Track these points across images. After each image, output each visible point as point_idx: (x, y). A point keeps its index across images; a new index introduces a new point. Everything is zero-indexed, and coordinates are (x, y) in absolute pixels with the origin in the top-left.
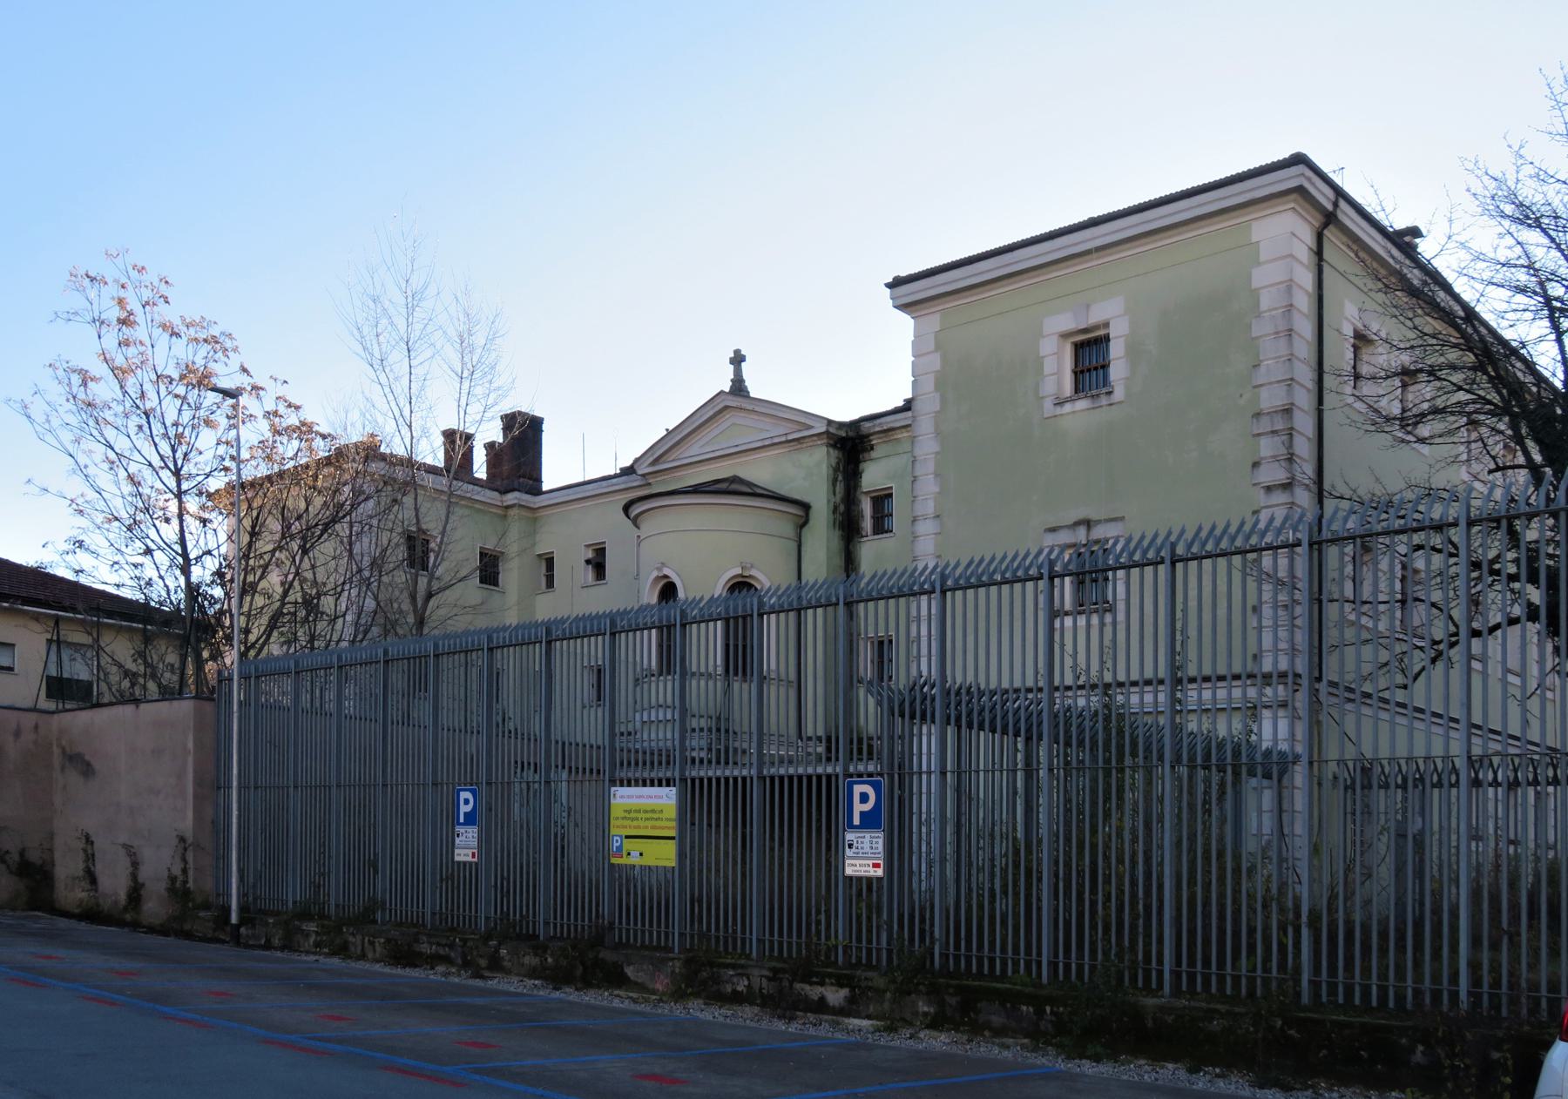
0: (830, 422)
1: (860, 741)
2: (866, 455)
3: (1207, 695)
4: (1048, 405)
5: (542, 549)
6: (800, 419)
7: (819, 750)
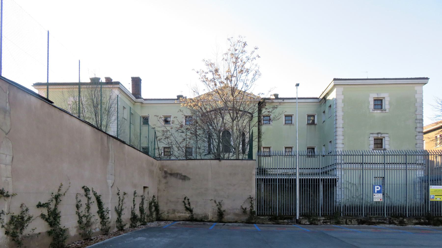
3: (400, 166)
4: (371, 111)
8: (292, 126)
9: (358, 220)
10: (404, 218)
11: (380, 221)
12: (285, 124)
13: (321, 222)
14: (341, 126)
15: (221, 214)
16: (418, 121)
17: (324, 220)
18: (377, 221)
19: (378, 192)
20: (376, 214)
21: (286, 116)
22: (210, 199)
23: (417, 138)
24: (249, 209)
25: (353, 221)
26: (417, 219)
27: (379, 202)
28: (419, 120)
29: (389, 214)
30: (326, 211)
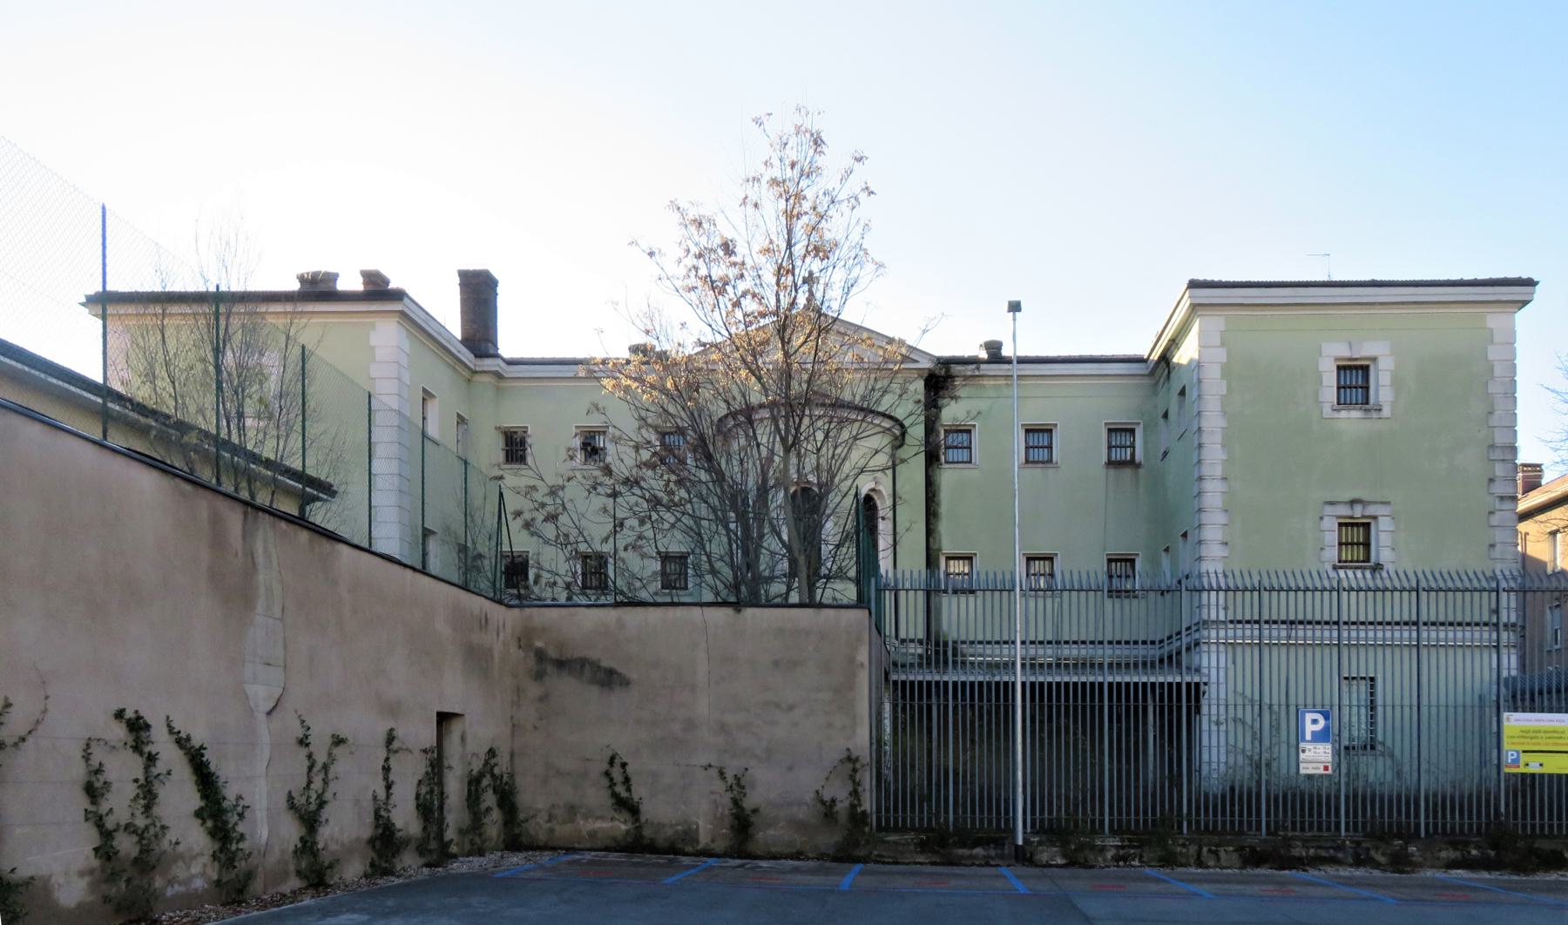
5: (512, 422)
6: (910, 354)
8: (1051, 472)
9: (1242, 848)
10: (1407, 843)
11: (1323, 853)
12: (1027, 461)
13: (1109, 855)
14: (1218, 471)
15: (742, 823)
16: (1497, 455)
17: (1117, 847)
18: (1312, 851)
20: (1311, 824)
22: (704, 762)
23: (1495, 520)
24: (847, 803)
25: (1222, 854)
26: (1454, 845)
28: (1504, 448)
29: (1356, 824)
30: (1128, 814)
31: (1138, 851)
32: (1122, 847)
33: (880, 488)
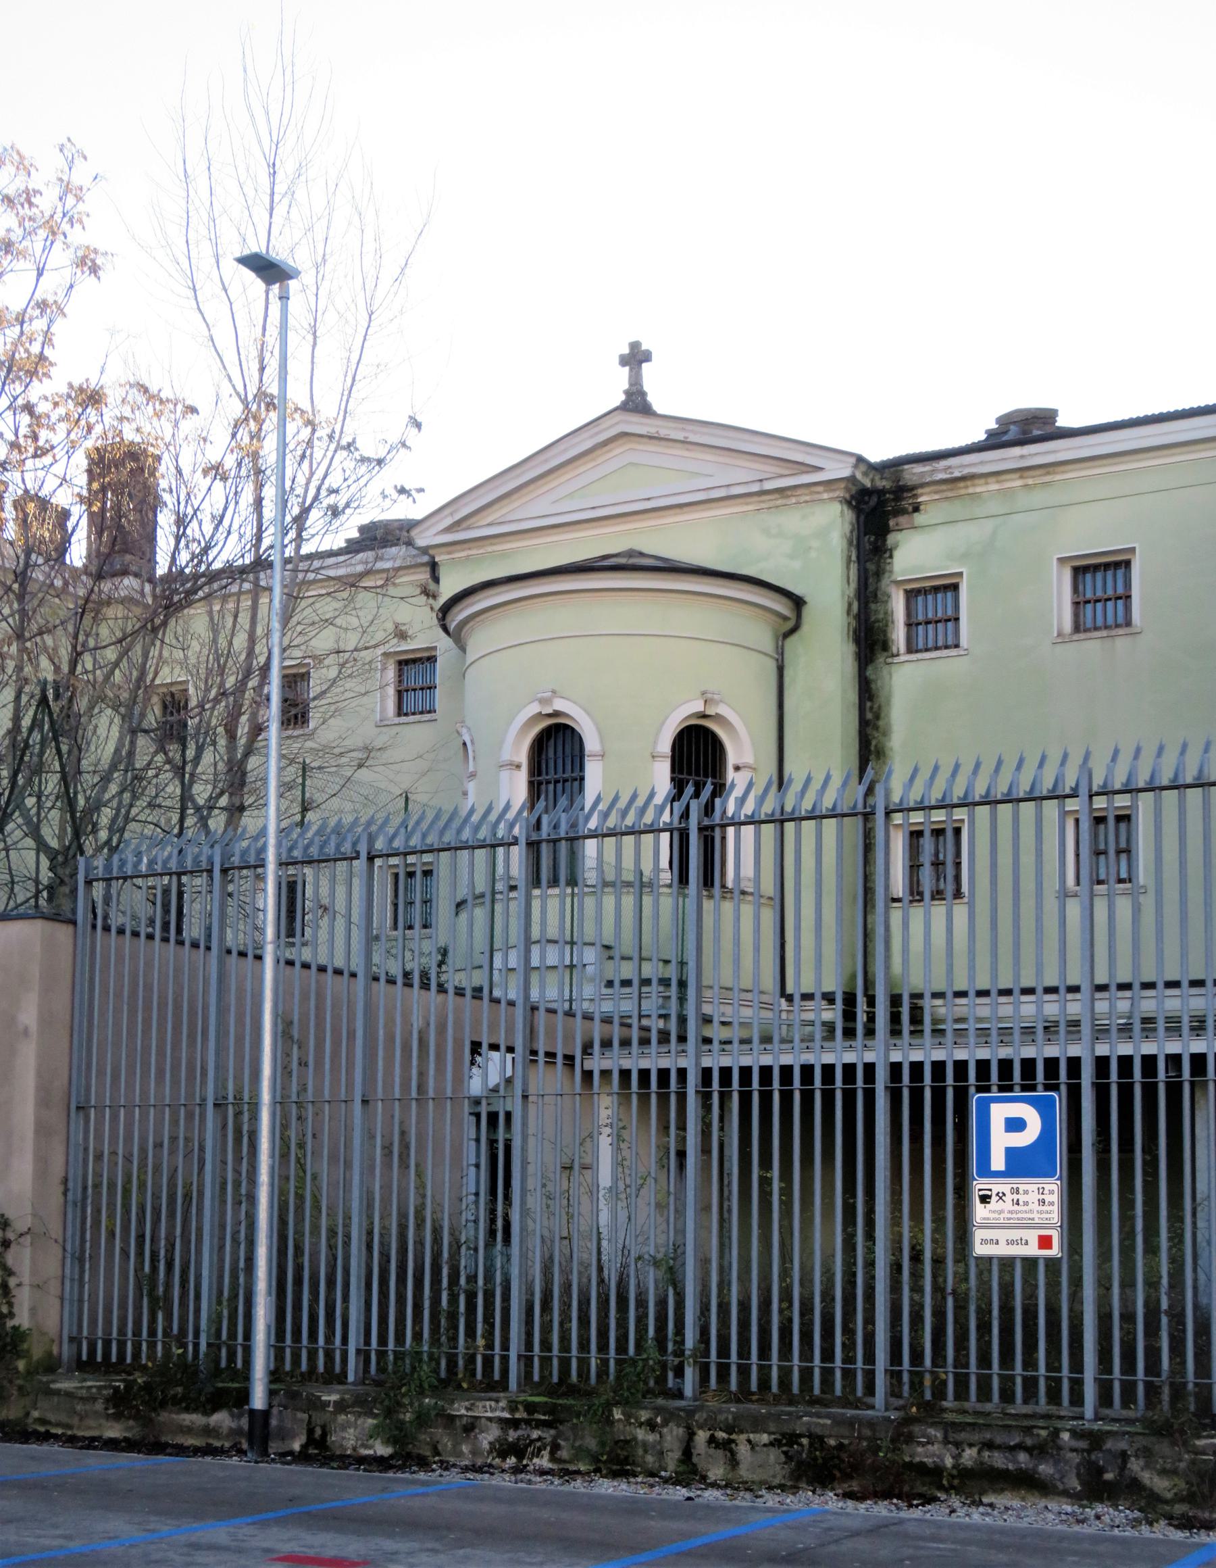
0: (860, 460)
1: (895, 1000)
2: (902, 520)
7: (827, 1016)
11: (998, 1460)
13: (487, 1438)
17: (506, 1424)
18: (969, 1455)
19: (1022, 1164)
20: (1030, 1385)
21: (1082, 571)
25: (743, 1450)
27: (1030, 1263)
31: (548, 1435)
32: (515, 1424)
33: (722, 710)
